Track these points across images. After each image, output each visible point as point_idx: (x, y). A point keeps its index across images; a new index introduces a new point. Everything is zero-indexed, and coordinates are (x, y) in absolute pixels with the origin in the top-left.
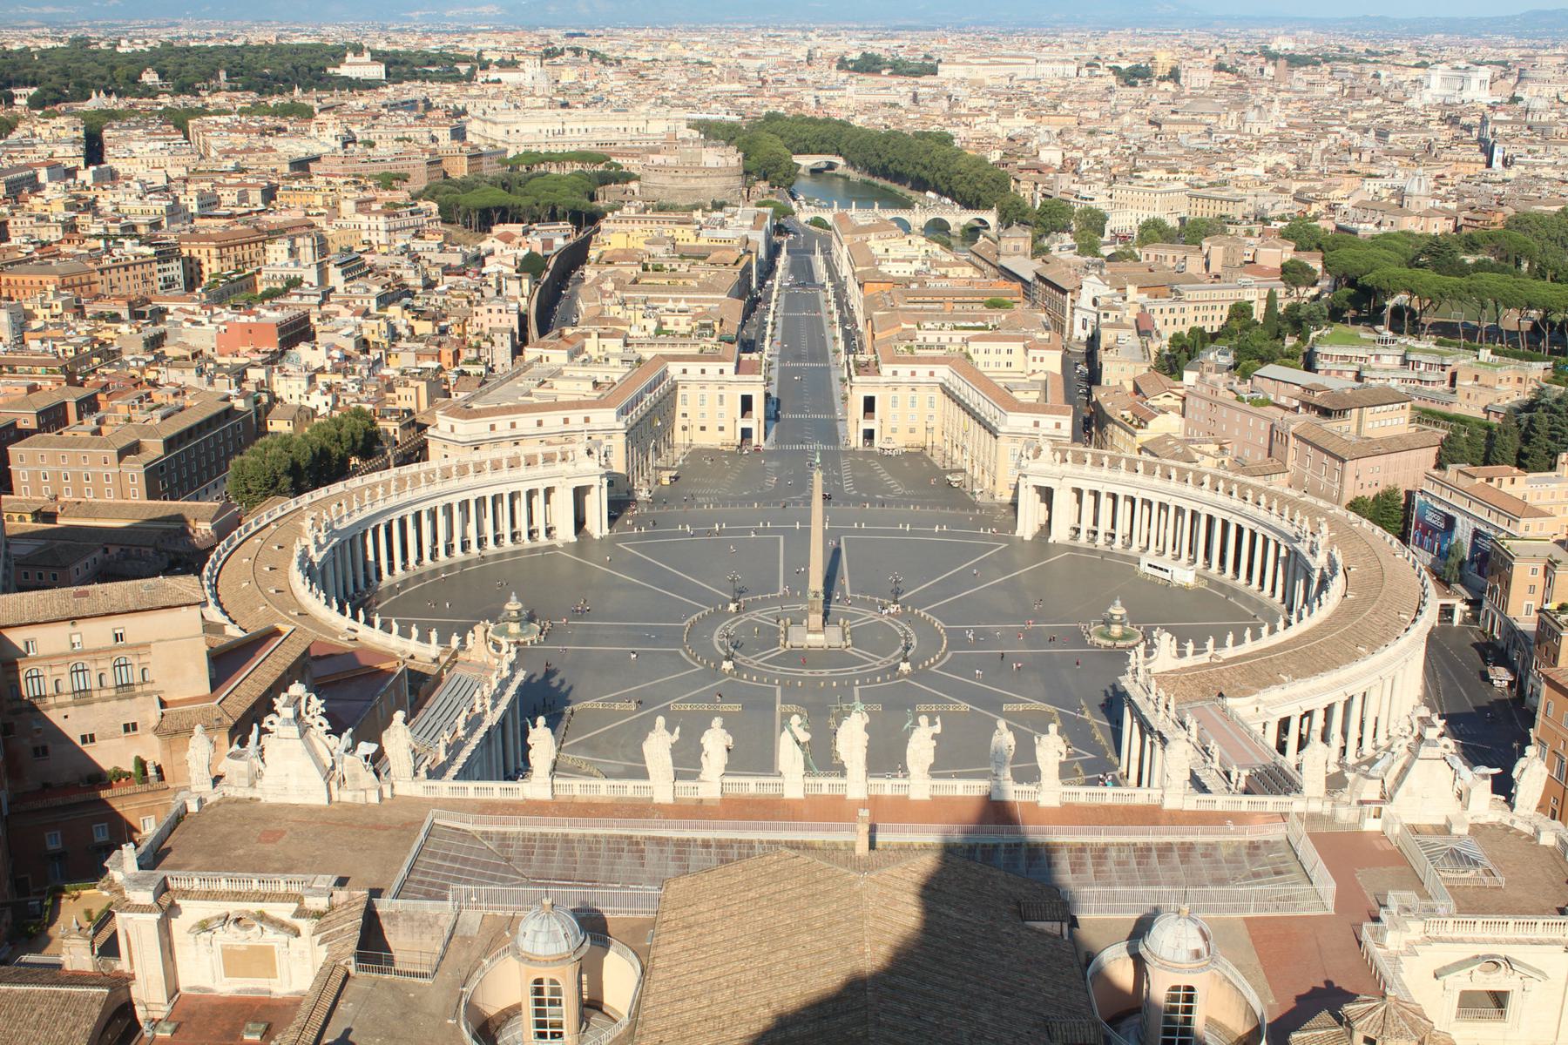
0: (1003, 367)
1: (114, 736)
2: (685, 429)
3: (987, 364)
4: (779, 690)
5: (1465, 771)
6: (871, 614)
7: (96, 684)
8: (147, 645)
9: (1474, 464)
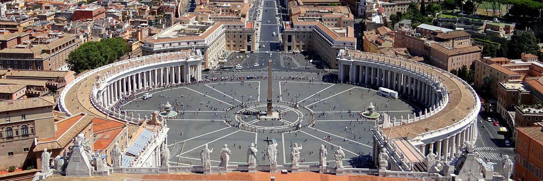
0: (334, 25)
1: (21, 152)
2: (229, 46)
3: (328, 24)
4: (257, 133)
5: (484, 164)
6: (289, 108)
7: (15, 135)
8: (34, 121)
9: (492, 57)
